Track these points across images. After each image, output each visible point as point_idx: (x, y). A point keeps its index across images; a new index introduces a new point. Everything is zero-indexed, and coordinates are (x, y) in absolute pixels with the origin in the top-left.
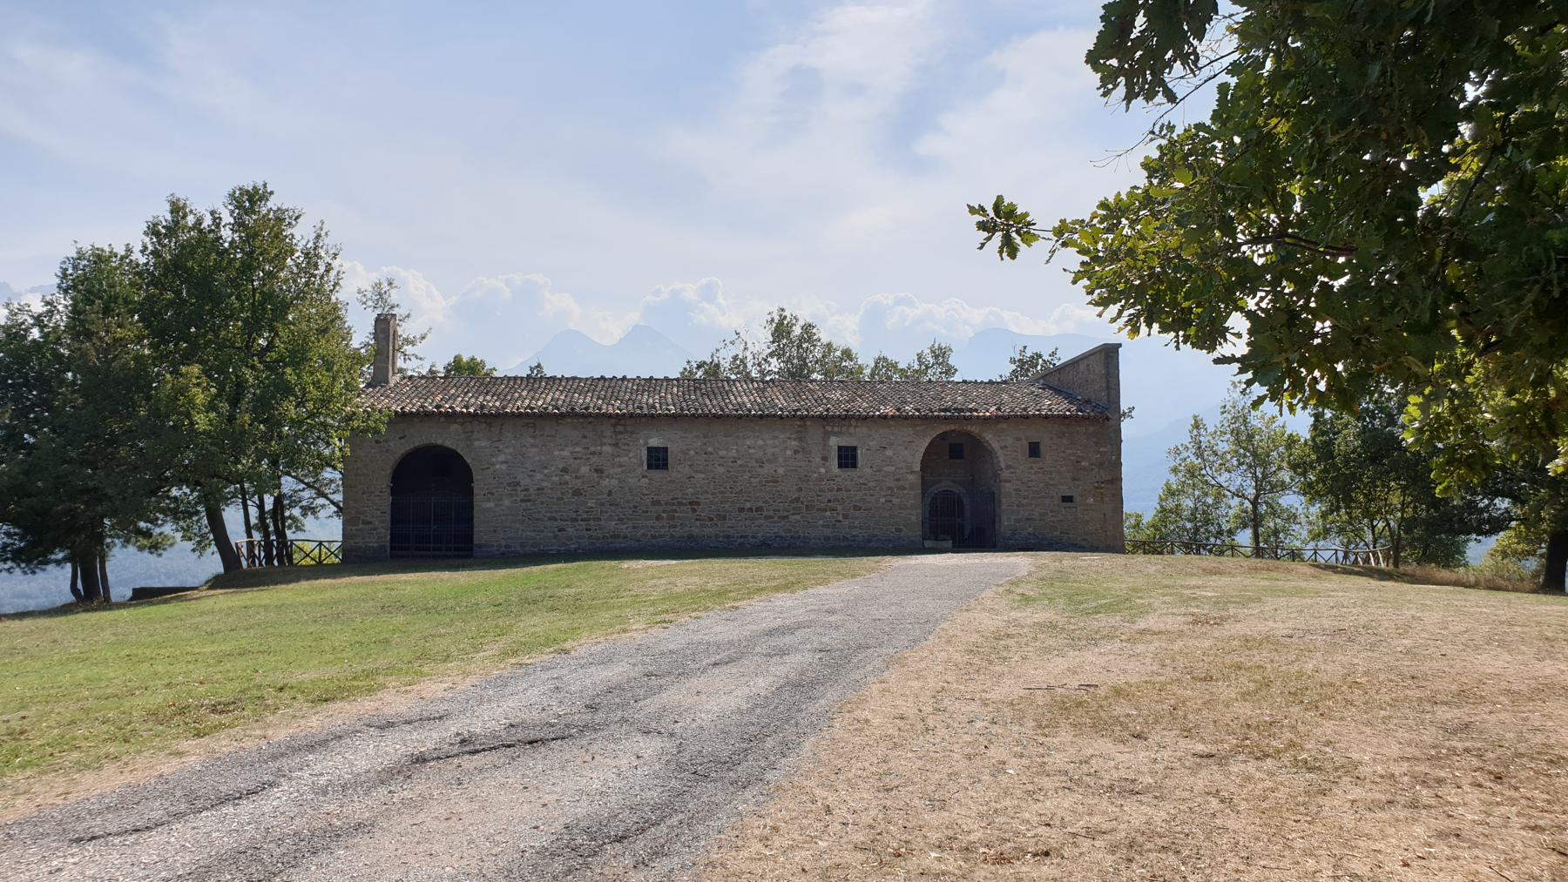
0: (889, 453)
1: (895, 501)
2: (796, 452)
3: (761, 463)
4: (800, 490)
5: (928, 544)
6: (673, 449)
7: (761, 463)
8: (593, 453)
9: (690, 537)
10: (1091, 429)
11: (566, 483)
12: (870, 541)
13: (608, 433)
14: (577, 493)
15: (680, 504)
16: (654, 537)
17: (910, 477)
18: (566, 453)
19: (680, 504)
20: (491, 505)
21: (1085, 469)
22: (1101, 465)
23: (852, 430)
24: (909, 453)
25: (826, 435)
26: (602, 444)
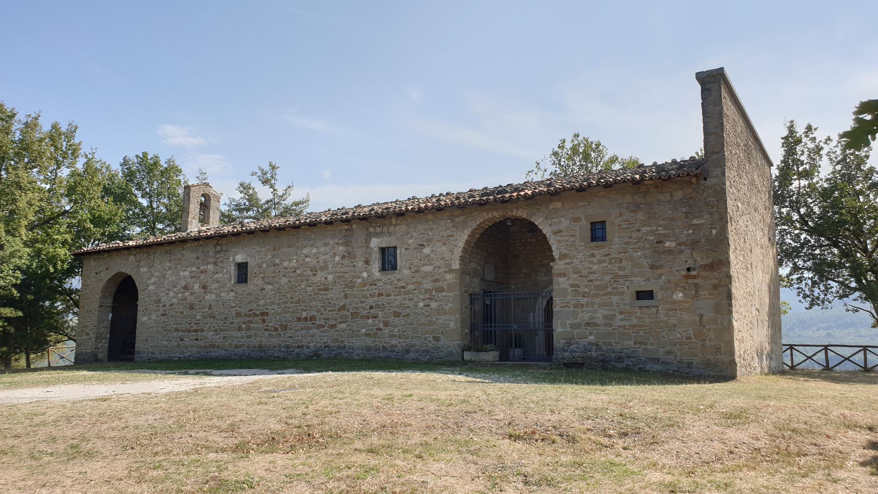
0: (427, 250)
1: (434, 305)
2: (343, 257)
3: (314, 270)
4: (346, 297)
5: (468, 356)
6: (252, 263)
7: (314, 270)
8: (202, 272)
9: (260, 347)
10: (679, 195)
11: (186, 299)
12: (408, 352)
13: (211, 254)
14: (192, 307)
15: (255, 315)
16: (236, 347)
17: (449, 276)
18: (187, 273)
19: (255, 315)
20: (145, 319)
21: (670, 251)
22: (694, 244)
23: (392, 228)
24: (445, 253)
25: (369, 237)
26: (208, 263)
